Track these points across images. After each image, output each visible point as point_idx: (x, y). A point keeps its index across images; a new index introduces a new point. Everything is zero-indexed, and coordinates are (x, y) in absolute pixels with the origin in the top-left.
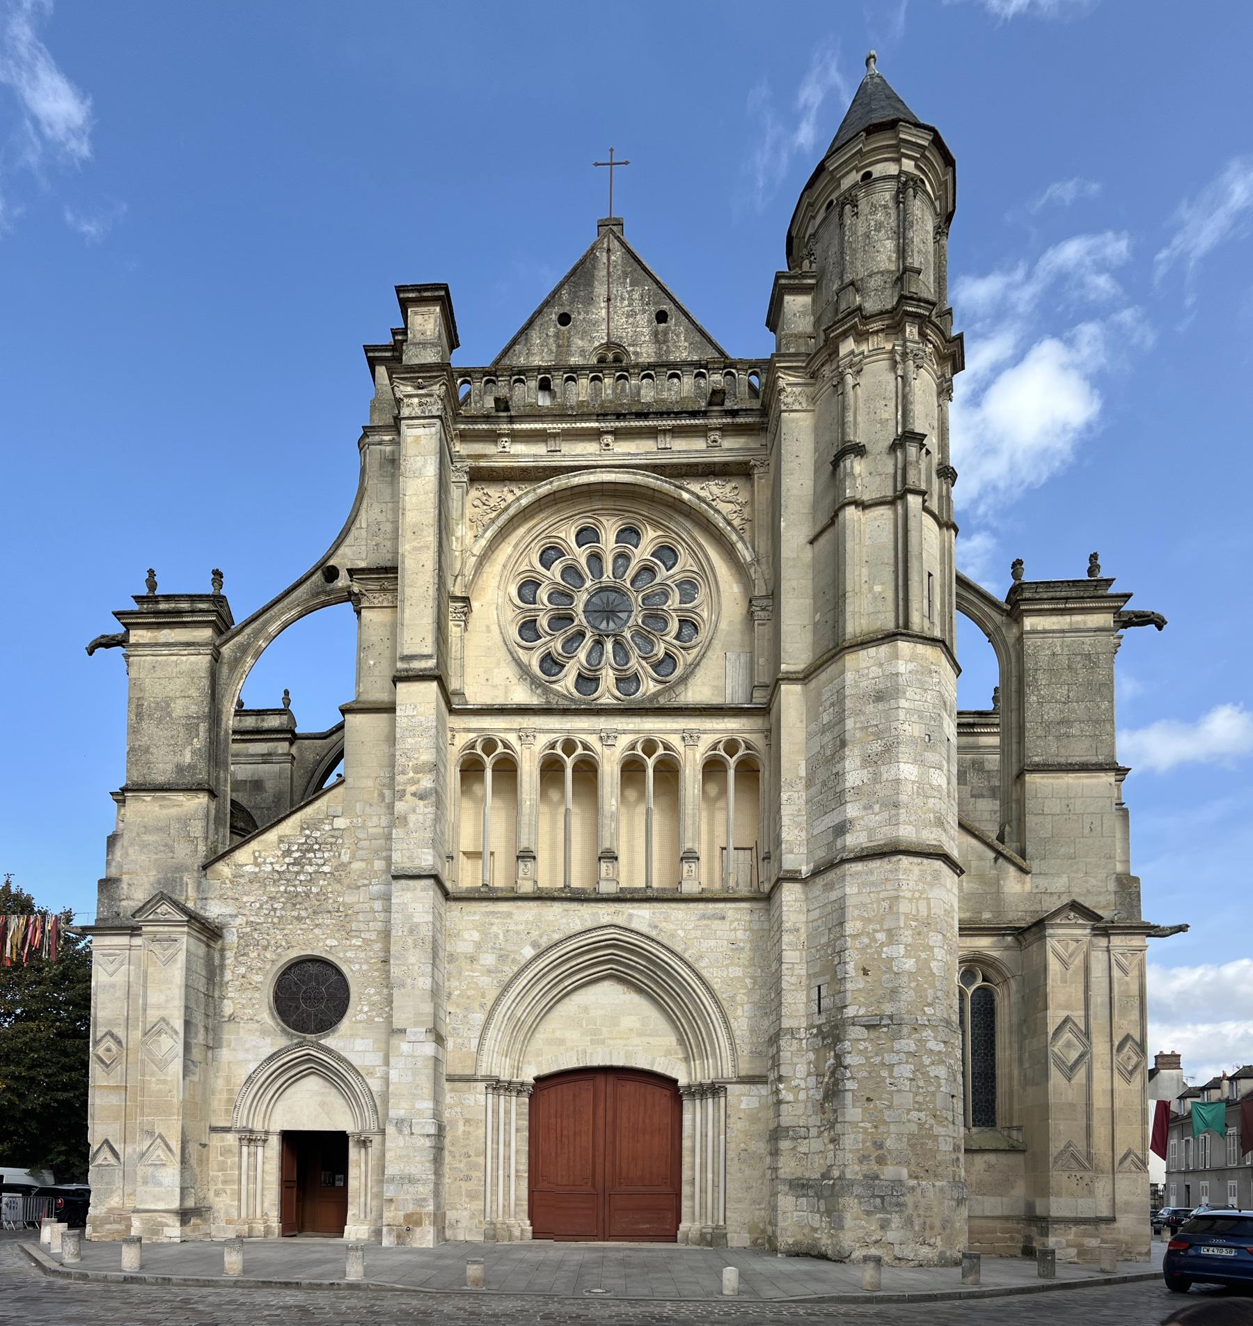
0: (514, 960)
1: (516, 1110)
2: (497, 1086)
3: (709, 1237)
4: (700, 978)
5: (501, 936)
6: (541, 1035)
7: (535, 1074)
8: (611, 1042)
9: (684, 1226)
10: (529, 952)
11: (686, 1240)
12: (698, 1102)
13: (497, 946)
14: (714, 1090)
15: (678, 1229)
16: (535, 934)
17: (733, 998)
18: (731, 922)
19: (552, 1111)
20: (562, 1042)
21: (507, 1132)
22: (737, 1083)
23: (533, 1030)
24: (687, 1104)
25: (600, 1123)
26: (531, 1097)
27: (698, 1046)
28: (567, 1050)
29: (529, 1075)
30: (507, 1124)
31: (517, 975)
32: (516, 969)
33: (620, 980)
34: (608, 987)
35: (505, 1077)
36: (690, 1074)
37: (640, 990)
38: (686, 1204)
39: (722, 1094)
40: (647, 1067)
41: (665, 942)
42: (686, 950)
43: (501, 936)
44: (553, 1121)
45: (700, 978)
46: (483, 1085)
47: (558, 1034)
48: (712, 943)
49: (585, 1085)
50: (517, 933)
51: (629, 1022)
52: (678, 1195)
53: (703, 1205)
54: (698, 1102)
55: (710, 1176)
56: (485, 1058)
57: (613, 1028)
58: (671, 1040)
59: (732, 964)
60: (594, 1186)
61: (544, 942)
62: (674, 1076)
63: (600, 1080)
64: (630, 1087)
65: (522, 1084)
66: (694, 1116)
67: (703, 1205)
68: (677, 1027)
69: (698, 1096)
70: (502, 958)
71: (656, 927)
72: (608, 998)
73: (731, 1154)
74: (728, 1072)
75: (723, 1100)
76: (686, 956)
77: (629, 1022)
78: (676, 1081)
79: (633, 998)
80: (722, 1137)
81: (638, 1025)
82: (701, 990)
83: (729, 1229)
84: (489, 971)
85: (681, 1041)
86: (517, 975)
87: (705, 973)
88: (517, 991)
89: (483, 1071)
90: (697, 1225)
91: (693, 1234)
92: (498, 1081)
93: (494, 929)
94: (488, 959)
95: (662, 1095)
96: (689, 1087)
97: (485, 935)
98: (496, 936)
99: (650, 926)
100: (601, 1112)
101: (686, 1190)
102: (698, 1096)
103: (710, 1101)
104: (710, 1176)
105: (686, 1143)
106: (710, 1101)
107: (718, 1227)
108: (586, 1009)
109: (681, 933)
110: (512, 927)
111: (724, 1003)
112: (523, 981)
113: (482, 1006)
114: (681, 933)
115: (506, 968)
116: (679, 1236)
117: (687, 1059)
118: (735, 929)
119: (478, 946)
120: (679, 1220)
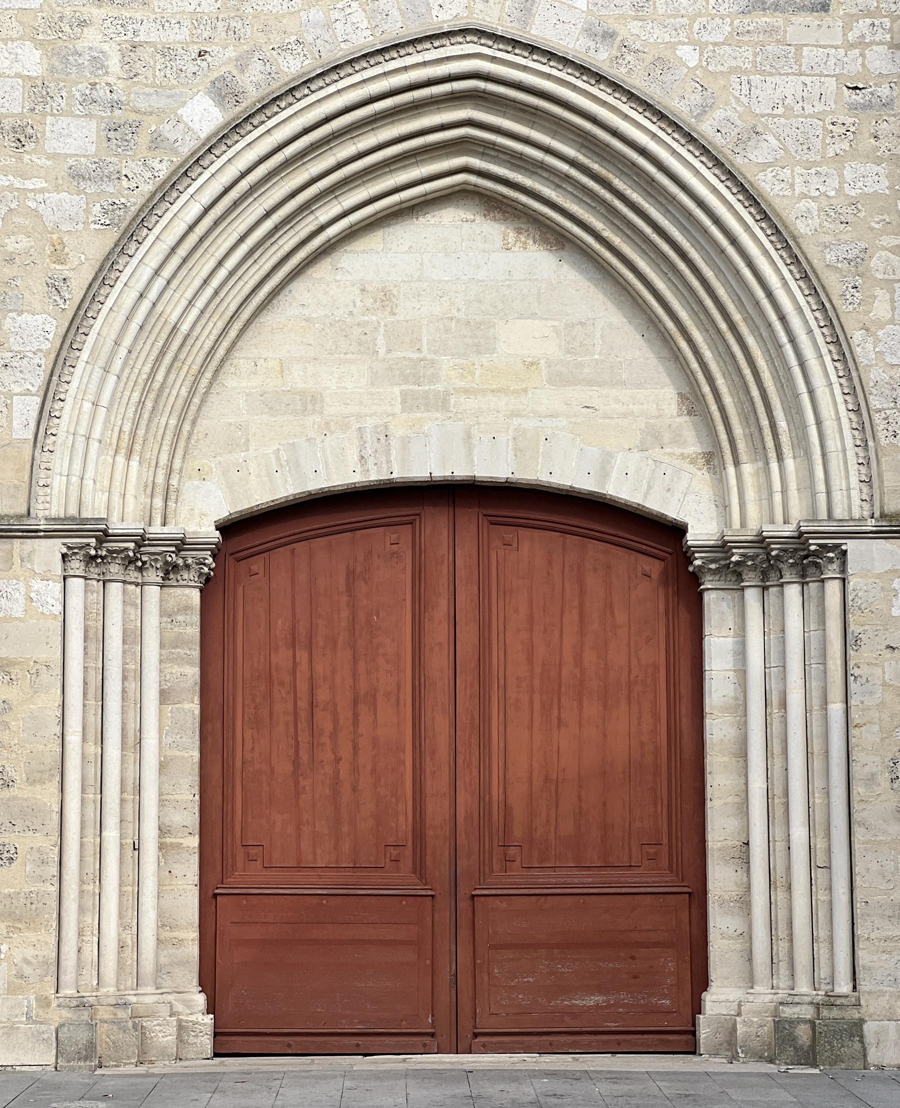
0: (157, 142)
1: (162, 621)
2: (98, 550)
3: (803, 1033)
4: (752, 198)
5: (114, 63)
6: (241, 381)
7: (224, 510)
8: (471, 403)
9: (719, 999)
10: (204, 116)
11: (730, 1045)
12: (752, 596)
13: (102, 93)
14: (802, 557)
15: (697, 1008)
16: (223, 57)
17: (858, 263)
18: (850, 20)
19: (281, 625)
20: (311, 401)
21: (133, 702)
22: (878, 534)
23: (217, 362)
24: (717, 605)
25: (437, 663)
26: (207, 586)
27: (749, 415)
28: (326, 429)
29: (200, 515)
30: (134, 675)
31: (168, 190)
32: (163, 170)
33: (494, 205)
34: (450, 221)
35: (126, 520)
36: (724, 506)
37: (556, 238)
38: (721, 925)
39: (832, 571)
40: (586, 484)
41: (637, 83)
42: (704, 110)
43: (114, 63)
44: (282, 658)
45: (752, 198)
46: (56, 547)
47: (297, 379)
48: (791, 87)
49: (385, 548)
50: (167, 52)
51: (523, 339)
52: (697, 898)
53: (780, 927)
54: (752, 596)
55: (799, 833)
56: (59, 462)
57: (480, 359)
58: (662, 396)
59: (854, 153)
60: (420, 869)
61: (254, 85)
62: (672, 511)
63: (436, 524)
64: (530, 550)
65: (181, 545)
66: (737, 637)
67: (780, 927)
68: (676, 356)
69: (751, 579)
70: (119, 133)
71: (609, 36)
72: (456, 257)
73: (867, 763)
74: (849, 501)
75: (833, 589)
76: (706, 129)
77: (523, 339)
78: (678, 530)
79: (538, 263)
80: (836, 708)
81: (552, 349)
82: (755, 241)
83: (872, 1006)
84: (77, 176)
85: (693, 402)
86: (168, 190)
87: (767, 184)
88: (171, 238)
89: (52, 505)
90: (763, 996)
91: (753, 1025)
92: (104, 536)
93: (91, 38)
94: (73, 136)
95: (636, 577)
96: (724, 547)
97: (61, 57)
98: (98, 62)
99: (589, 31)
100: (438, 631)
101: (721, 879)
102: (751, 579)
103: (793, 592)
104: (799, 833)
105: (718, 729)
106: (793, 592)
107: (831, 1001)
108: (385, 298)
109: (688, 55)
110: (148, 33)
111: (833, 282)
112: (187, 208)
113: (56, 286)
114: (688, 55)
115: (131, 167)
116: (704, 1032)
117: (712, 459)
118: (861, 44)
119: (40, 92)
120: (701, 982)
